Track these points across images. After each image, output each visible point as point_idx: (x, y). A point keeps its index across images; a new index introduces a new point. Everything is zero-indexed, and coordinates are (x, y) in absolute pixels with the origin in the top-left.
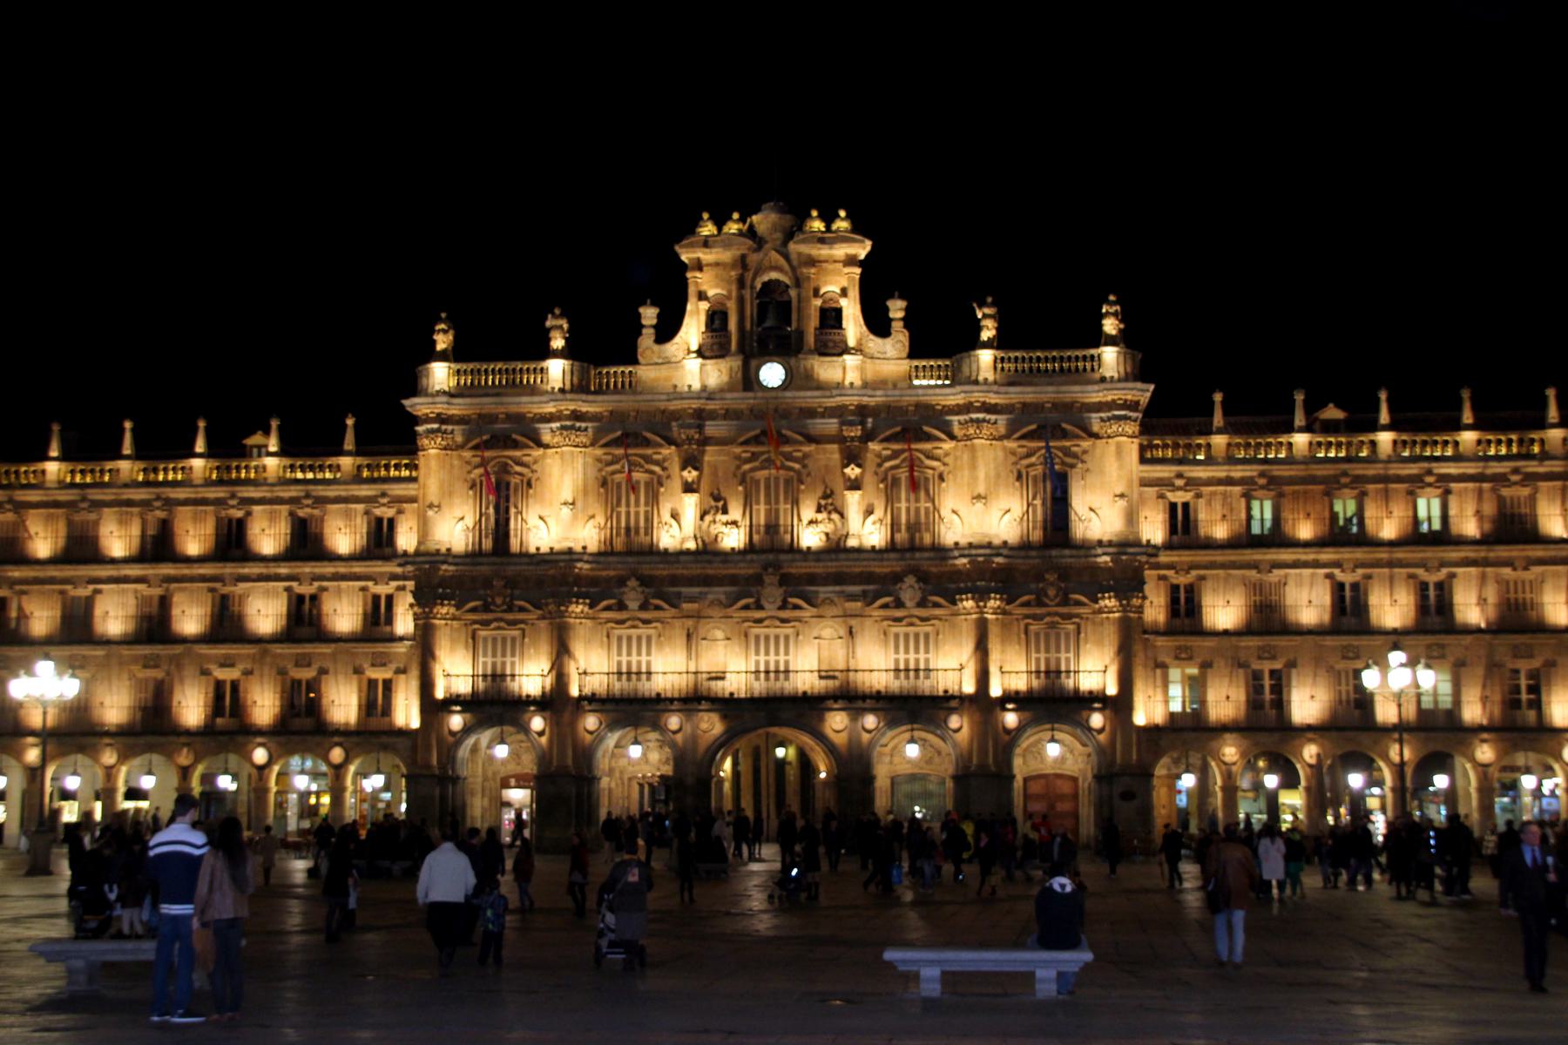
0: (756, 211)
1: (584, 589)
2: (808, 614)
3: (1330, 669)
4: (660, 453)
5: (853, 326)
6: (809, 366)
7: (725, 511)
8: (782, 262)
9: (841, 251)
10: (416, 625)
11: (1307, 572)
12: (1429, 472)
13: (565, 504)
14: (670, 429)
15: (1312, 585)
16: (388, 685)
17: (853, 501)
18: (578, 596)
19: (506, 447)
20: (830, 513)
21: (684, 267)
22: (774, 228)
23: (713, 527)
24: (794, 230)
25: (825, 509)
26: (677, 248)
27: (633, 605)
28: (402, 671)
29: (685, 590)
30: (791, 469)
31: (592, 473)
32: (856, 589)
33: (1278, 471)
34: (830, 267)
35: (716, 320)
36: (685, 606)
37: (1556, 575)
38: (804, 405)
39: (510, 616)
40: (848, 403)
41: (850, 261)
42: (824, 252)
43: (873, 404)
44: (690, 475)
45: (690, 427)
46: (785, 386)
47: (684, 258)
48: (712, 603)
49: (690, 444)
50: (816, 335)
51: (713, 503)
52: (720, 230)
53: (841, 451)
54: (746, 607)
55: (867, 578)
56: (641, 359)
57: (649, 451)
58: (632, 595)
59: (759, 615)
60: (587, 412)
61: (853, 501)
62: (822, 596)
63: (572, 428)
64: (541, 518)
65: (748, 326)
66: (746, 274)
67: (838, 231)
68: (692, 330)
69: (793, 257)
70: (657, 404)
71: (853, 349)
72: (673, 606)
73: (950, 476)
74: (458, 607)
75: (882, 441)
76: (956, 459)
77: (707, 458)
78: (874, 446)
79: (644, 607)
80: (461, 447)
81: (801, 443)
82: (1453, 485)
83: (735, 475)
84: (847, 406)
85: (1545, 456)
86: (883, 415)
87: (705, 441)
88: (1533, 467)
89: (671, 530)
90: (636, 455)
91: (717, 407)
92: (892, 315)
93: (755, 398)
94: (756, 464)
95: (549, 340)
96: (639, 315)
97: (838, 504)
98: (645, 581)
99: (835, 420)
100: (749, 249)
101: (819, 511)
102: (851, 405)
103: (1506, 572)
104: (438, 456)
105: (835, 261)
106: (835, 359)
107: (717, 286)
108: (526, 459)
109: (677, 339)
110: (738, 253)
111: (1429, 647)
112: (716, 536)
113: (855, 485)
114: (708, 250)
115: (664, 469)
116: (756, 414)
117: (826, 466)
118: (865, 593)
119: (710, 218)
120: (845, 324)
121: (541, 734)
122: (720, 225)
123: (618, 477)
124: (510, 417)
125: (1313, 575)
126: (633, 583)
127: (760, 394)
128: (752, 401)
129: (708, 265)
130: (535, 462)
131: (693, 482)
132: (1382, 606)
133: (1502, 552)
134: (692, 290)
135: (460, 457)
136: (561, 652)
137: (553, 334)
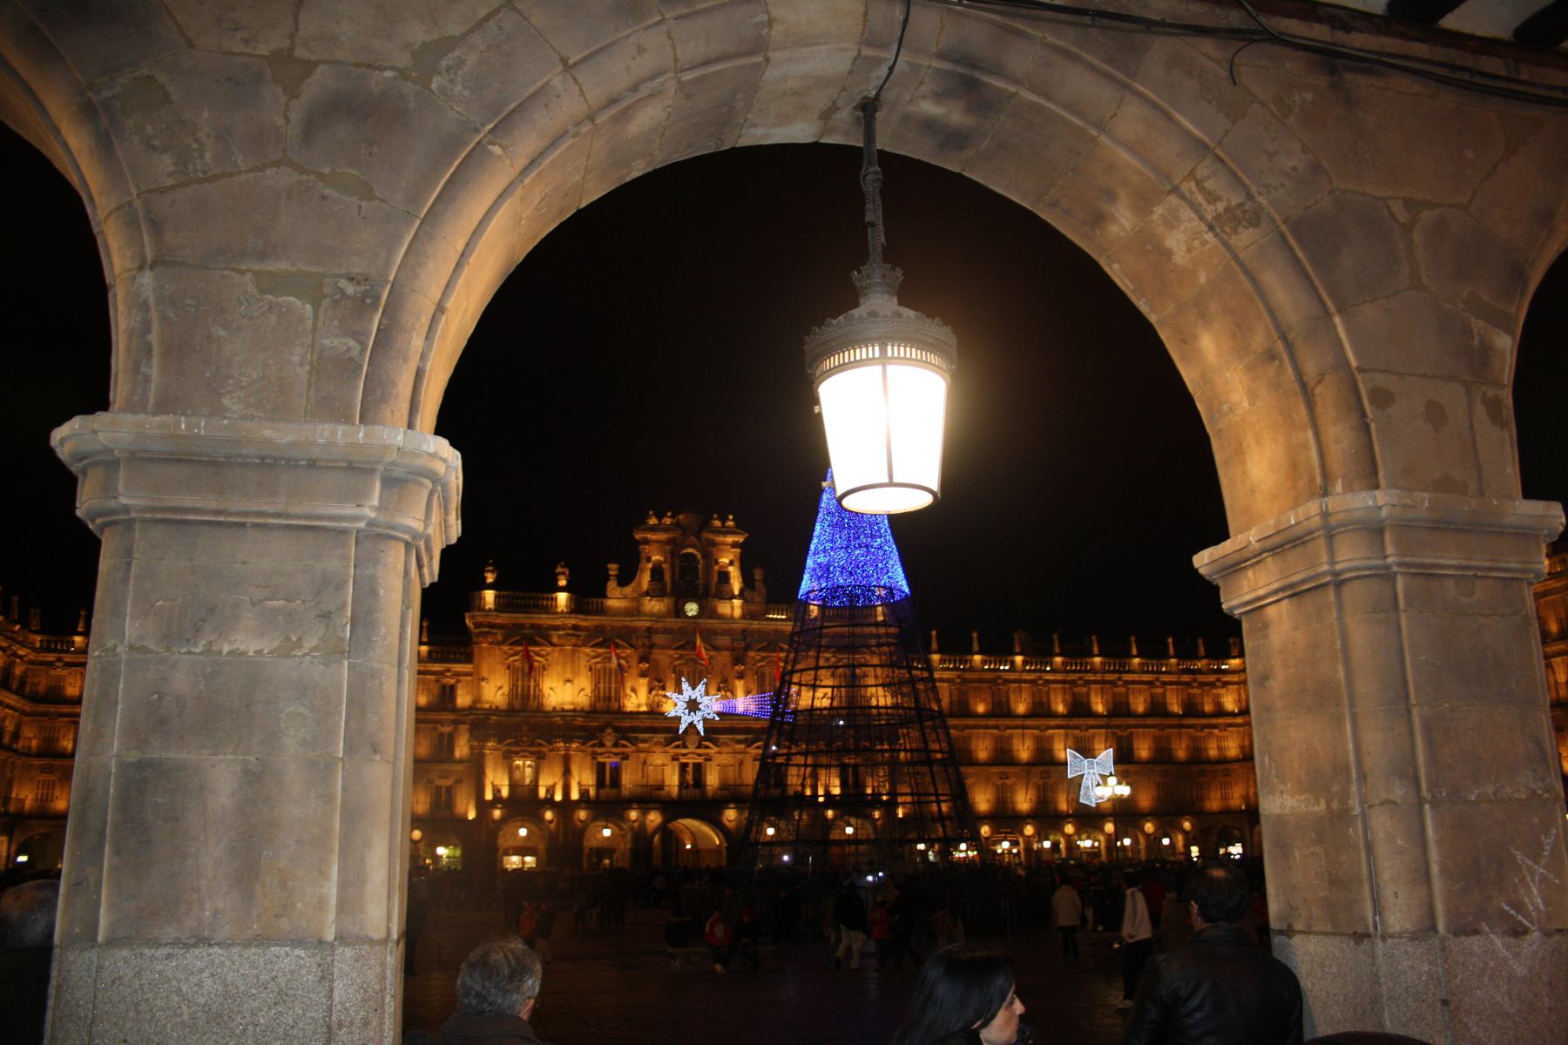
0: (678, 514)
1: (578, 734)
2: (712, 751)
3: (994, 784)
5: (736, 585)
7: (664, 688)
8: (698, 543)
9: (730, 539)
10: (472, 754)
11: (982, 731)
12: (1040, 678)
13: (569, 681)
15: (984, 738)
16: (449, 790)
17: (739, 686)
18: (576, 737)
19: (530, 645)
21: (638, 543)
24: (705, 524)
27: (609, 744)
28: (459, 781)
29: (641, 736)
31: (583, 663)
32: (742, 737)
33: (968, 675)
35: (657, 572)
36: (641, 745)
37: (1100, 734)
39: (532, 749)
41: (734, 545)
42: (720, 539)
46: (700, 615)
47: (638, 536)
48: (656, 744)
51: (657, 684)
52: (660, 521)
53: (732, 656)
54: (677, 747)
55: (747, 730)
56: (609, 594)
58: (609, 738)
59: (684, 751)
61: (739, 686)
62: (721, 741)
63: (573, 635)
64: (551, 689)
65: (677, 578)
67: (728, 527)
68: (645, 580)
72: (633, 745)
74: (499, 743)
77: (652, 657)
78: (751, 654)
79: (616, 745)
80: (503, 643)
82: (1052, 686)
85: (1093, 671)
86: (756, 636)
87: (652, 646)
88: (1090, 677)
94: (682, 661)
95: (557, 581)
96: (608, 570)
97: (730, 686)
98: (616, 729)
99: (728, 638)
101: (719, 690)
103: (1077, 731)
104: (487, 648)
107: (657, 554)
108: (543, 652)
110: (671, 536)
111: (1042, 772)
113: (741, 676)
115: (627, 662)
116: (681, 631)
118: (746, 739)
119: (654, 514)
120: (732, 581)
121: (551, 822)
122: (660, 518)
123: (599, 666)
124: (533, 626)
125: (985, 733)
126: (609, 731)
127: (686, 620)
129: (653, 541)
130: (548, 654)
132: (1018, 750)
133: (1076, 721)
134: (643, 556)
135: (500, 649)
136: (567, 773)
137: (560, 577)
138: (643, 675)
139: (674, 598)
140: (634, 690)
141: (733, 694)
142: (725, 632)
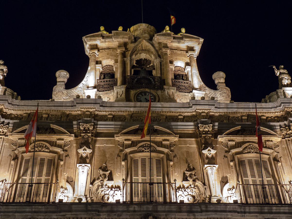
4: (63, 139)
6: (171, 93)
8: (150, 47)
9: (184, 45)
14: (72, 127)
20: (194, 181)
22: (144, 32)
23: (100, 190)
25: (191, 176)
26: (84, 38)
30: (162, 152)
34: (179, 52)
38: (169, 114)
40: (201, 111)
43: (217, 114)
44: (85, 152)
45: (87, 122)
49: (86, 132)
50: (172, 82)
51: (101, 172)
53: (197, 143)
57: (54, 138)
60: (11, 114)
66: (127, 53)
67: (181, 35)
69: (156, 45)
70: (63, 109)
71: (198, 89)
73: (282, 159)
75: (228, 134)
76: (283, 149)
78: (221, 139)
81: (169, 134)
83: (119, 156)
84: (200, 113)
86: (225, 121)
89: (66, 191)
90: (43, 141)
91: (107, 114)
92: (216, 82)
93: (135, 107)
97: (200, 176)
99: (192, 124)
100: (129, 39)
101: (185, 179)
102: (202, 112)
105: (181, 50)
106: (187, 94)
109: (81, 85)
110: (121, 40)
112: (103, 197)
114: (103, 40)
117: (188, 153)
128: (132, 109)
131: (87, 157)
138: (82, 160)
139: (125, 86)
140: (71, 182)
141: (204, 184)
142: (186, 119)
